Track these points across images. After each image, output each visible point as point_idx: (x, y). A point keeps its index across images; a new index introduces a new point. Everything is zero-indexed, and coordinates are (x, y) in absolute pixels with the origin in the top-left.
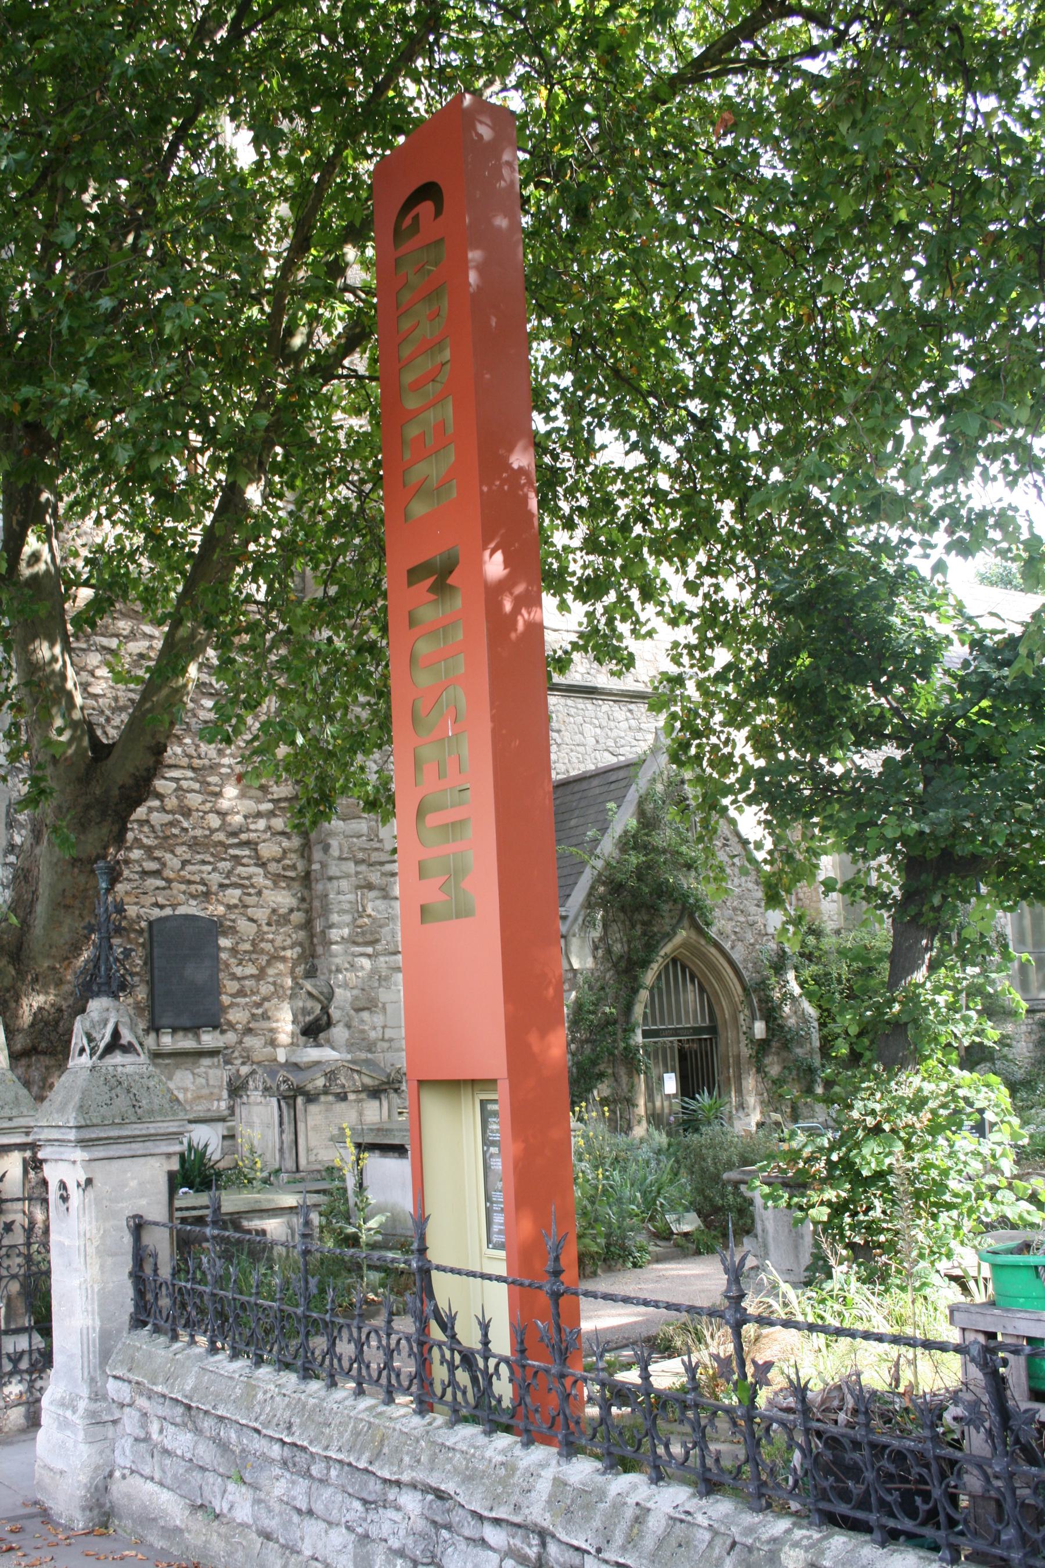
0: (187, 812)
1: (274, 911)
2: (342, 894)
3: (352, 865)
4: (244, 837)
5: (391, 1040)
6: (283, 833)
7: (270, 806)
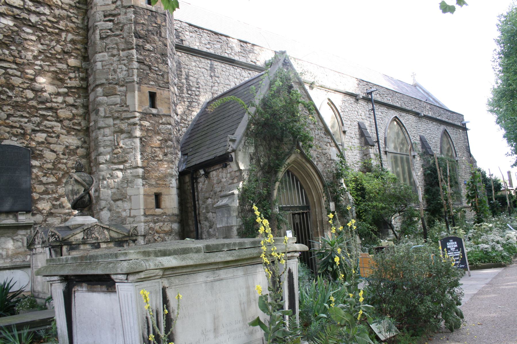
0: (12, 87)
1: (67, 147)
2: (105, 136)
4: (49, 105)
5: (134, 217)
6: (73, 105)
7: (66, 90)
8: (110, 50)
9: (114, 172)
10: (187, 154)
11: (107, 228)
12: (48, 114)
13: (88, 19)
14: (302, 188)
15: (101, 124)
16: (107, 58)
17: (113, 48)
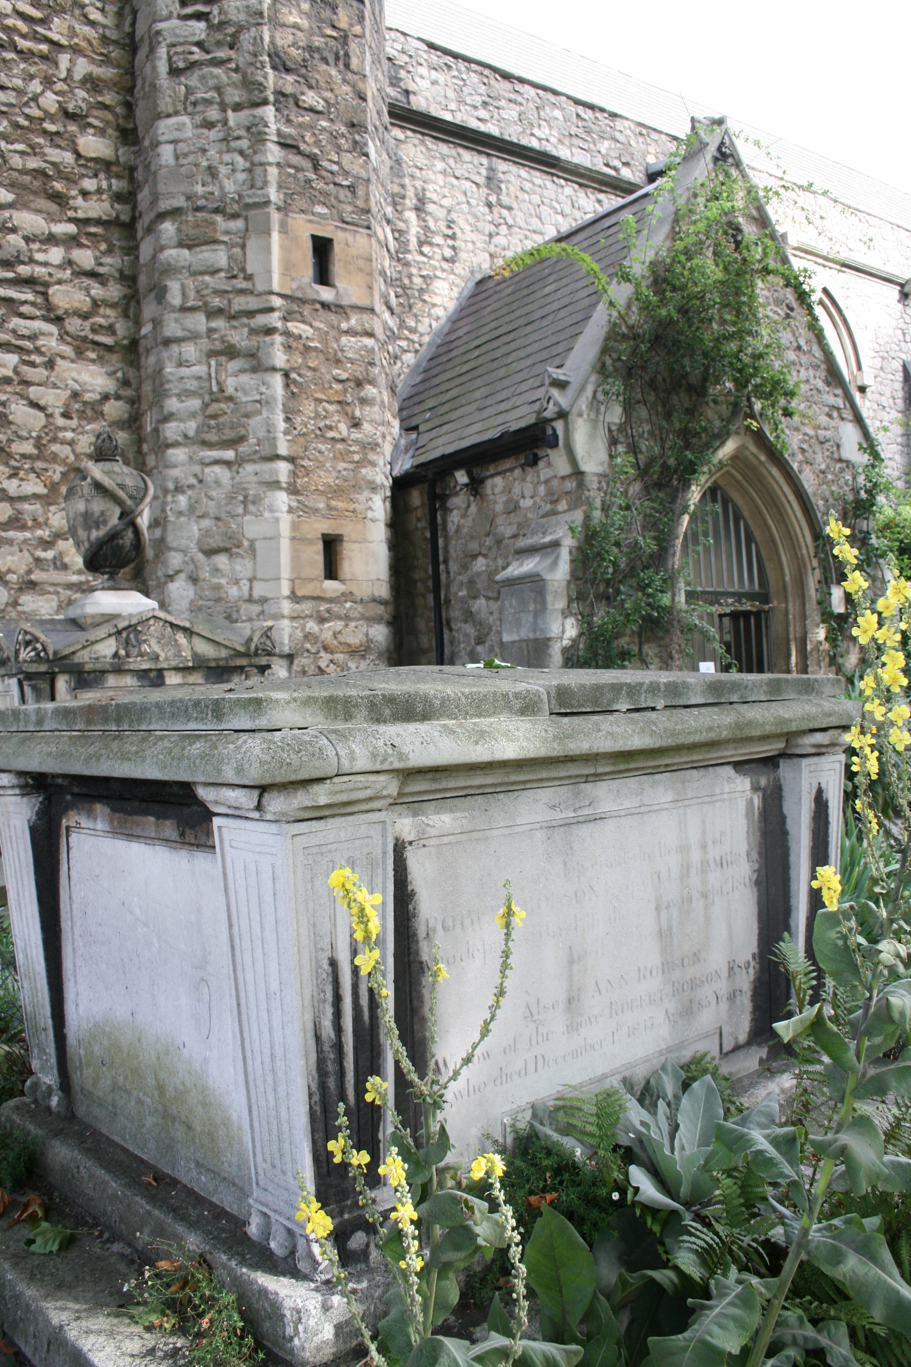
1: (75, 395)
2: (185, 367)
3: (201, 318)
4: (24, 270)
5: (263, 601)
6: (92, 274)
7: (72, 228)
8: (200, 108)
9: (207, 470)
10: (416, 428)
11: (185, 629)
12: (23, 297)
13: (135, 12)
14: (750, 539)
15: (172, 328)
16: (189, 132)
17: (208, 102)
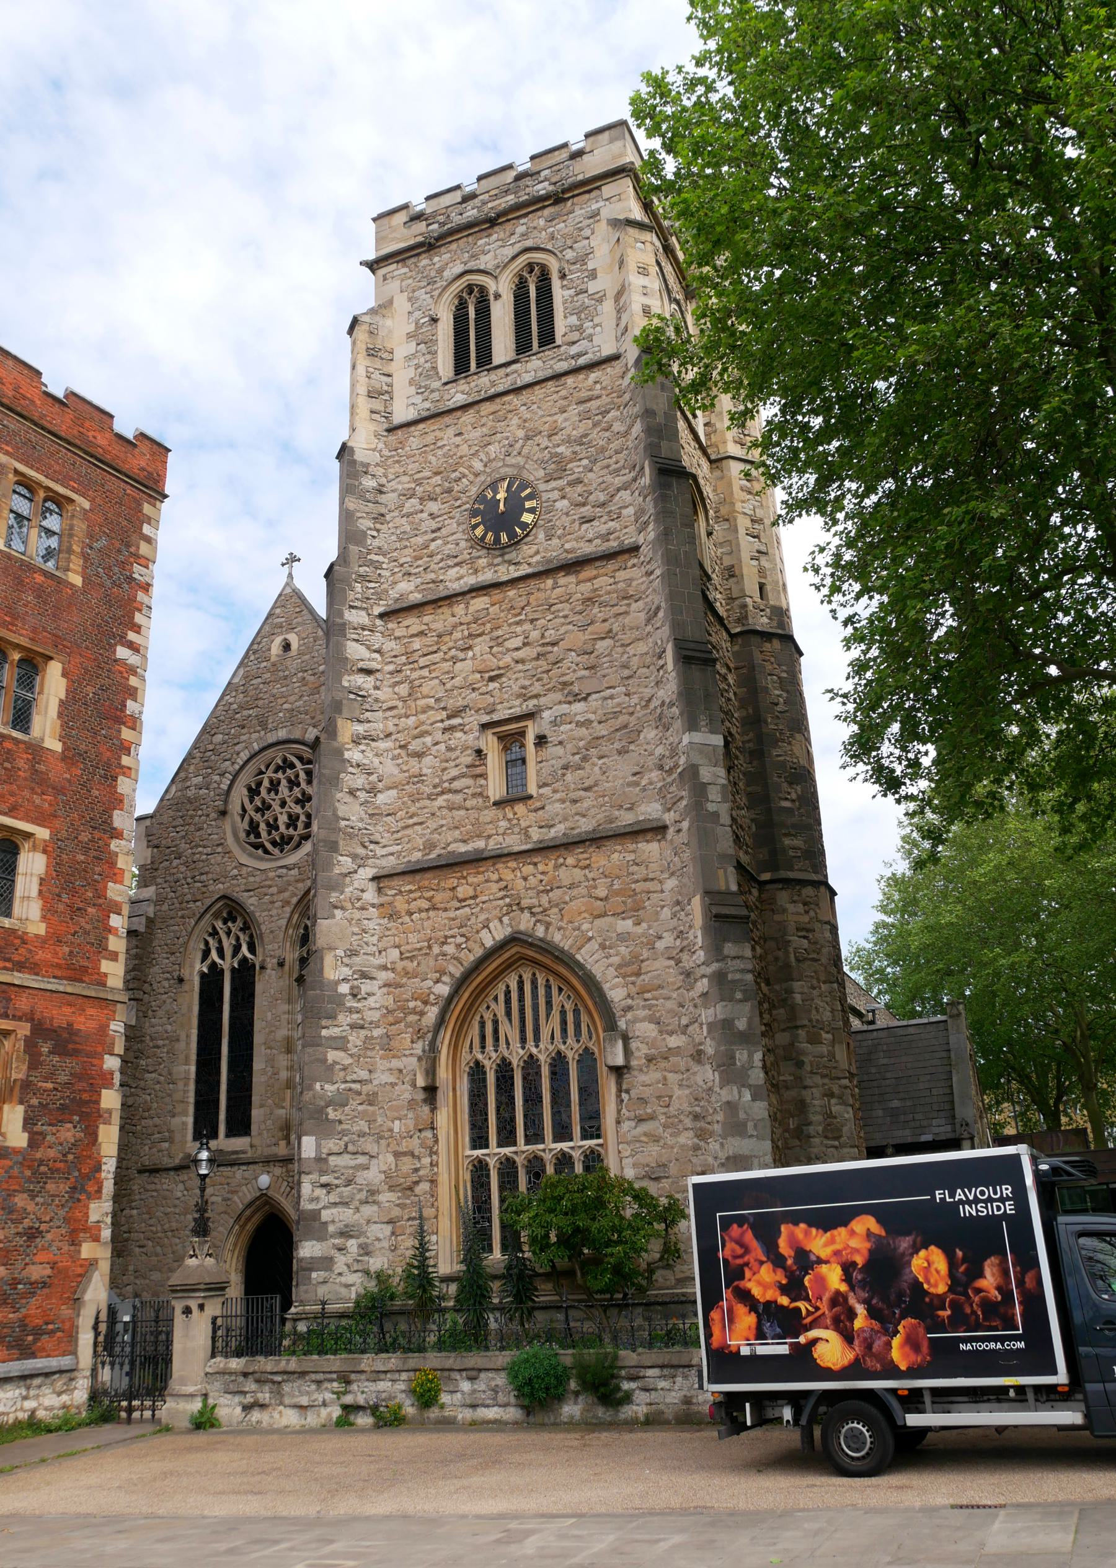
15: (808, 1082)
